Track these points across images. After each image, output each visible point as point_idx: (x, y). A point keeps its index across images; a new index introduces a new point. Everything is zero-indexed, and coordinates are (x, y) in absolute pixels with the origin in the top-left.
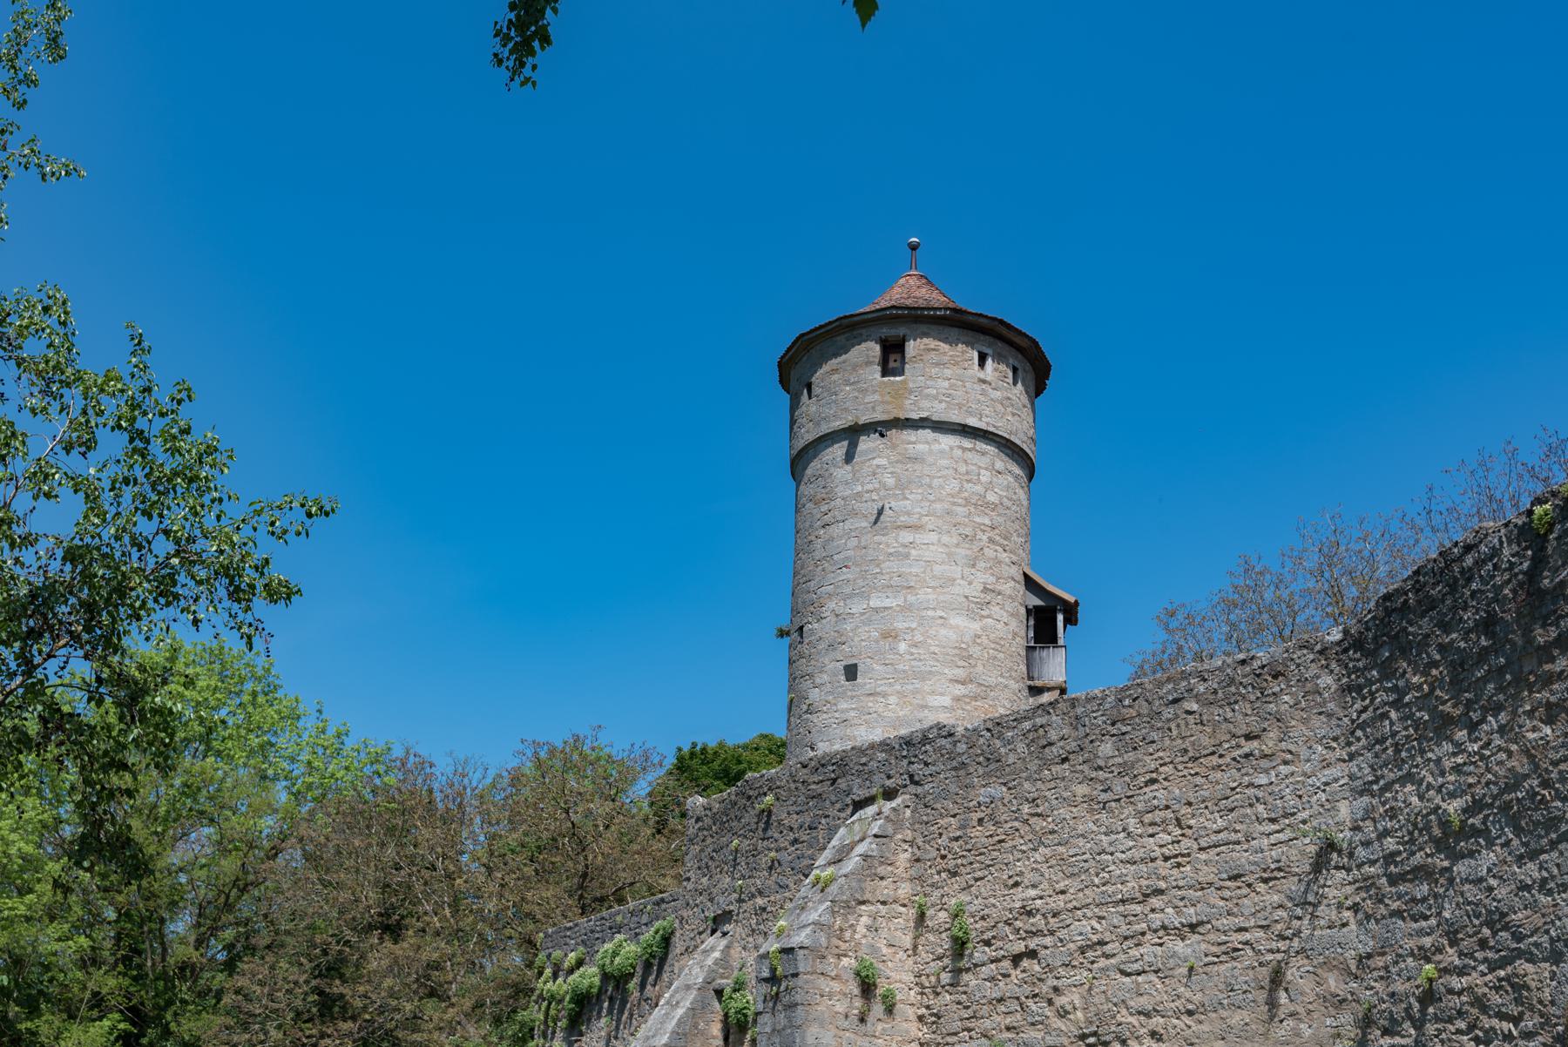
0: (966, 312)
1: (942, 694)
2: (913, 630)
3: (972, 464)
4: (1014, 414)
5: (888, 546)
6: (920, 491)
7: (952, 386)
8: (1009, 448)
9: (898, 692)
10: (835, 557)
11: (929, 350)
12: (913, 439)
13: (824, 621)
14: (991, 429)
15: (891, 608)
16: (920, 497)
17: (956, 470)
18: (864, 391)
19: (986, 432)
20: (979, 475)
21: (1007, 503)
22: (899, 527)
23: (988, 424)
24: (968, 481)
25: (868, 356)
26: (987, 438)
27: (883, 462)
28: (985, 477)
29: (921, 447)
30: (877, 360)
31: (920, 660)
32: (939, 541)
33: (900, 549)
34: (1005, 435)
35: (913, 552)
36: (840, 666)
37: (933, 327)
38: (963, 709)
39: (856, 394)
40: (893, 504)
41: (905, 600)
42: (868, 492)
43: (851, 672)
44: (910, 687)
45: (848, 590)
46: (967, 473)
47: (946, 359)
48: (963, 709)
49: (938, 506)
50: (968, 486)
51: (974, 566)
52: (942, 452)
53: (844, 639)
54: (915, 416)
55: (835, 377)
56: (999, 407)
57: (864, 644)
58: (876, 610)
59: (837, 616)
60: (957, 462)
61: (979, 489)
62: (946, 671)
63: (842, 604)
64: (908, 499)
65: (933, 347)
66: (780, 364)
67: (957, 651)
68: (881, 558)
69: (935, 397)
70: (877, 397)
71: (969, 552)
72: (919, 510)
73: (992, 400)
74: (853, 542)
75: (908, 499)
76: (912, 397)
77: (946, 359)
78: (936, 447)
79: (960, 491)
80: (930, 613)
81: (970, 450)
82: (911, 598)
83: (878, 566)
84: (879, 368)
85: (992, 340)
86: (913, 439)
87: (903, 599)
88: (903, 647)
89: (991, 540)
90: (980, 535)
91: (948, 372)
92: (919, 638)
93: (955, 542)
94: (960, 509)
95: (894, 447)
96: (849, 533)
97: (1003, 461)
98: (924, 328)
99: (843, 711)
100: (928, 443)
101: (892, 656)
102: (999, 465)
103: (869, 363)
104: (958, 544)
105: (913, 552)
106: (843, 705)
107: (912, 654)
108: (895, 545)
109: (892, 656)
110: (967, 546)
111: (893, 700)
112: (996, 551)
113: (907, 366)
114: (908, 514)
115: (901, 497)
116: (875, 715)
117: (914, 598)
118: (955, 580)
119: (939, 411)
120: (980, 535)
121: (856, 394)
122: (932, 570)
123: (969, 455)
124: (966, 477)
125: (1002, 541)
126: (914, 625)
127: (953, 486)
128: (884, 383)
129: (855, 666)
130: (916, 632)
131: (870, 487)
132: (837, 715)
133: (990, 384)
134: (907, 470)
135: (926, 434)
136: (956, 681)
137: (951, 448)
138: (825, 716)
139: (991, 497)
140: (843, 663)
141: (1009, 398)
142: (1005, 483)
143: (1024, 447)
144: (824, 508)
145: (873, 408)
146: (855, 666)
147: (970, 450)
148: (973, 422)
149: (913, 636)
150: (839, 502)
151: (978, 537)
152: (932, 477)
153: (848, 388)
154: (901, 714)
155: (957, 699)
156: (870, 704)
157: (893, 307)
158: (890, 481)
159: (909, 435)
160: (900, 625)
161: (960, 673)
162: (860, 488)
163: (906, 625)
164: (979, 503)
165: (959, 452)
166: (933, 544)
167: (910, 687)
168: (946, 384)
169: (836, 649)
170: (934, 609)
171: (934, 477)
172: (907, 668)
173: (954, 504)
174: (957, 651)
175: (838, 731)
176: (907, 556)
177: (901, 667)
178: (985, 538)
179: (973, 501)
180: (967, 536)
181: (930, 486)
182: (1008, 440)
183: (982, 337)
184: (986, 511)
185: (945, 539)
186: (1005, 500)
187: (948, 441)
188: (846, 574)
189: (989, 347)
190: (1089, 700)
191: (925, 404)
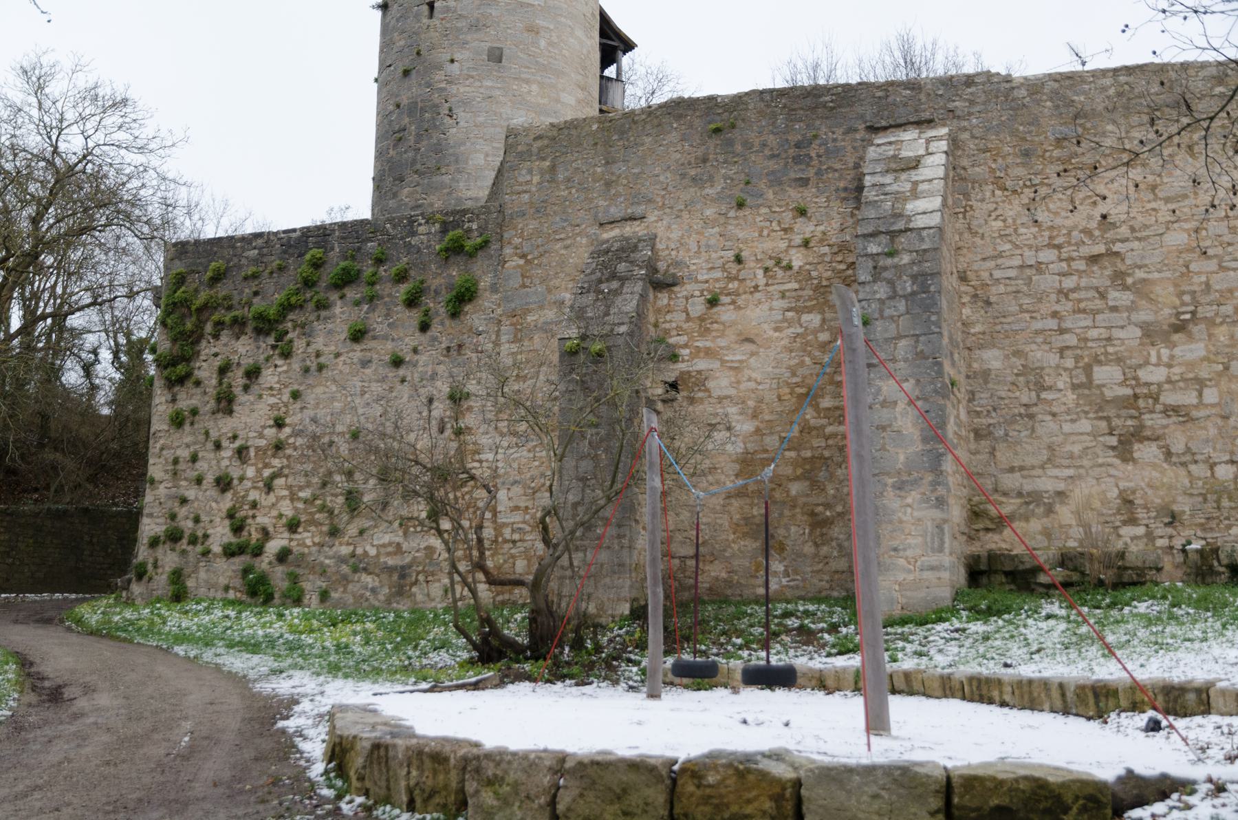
36: (486, 46)
43: (496, 56)
80: (563, 20)
92: (555, 39)
99: (487, 88)
106: (489, 83)
111: (534, 87)
129: (501, 49)
132: (482, 90)
140: (489, 44)
146: (501, 49)
154: (541, 101)
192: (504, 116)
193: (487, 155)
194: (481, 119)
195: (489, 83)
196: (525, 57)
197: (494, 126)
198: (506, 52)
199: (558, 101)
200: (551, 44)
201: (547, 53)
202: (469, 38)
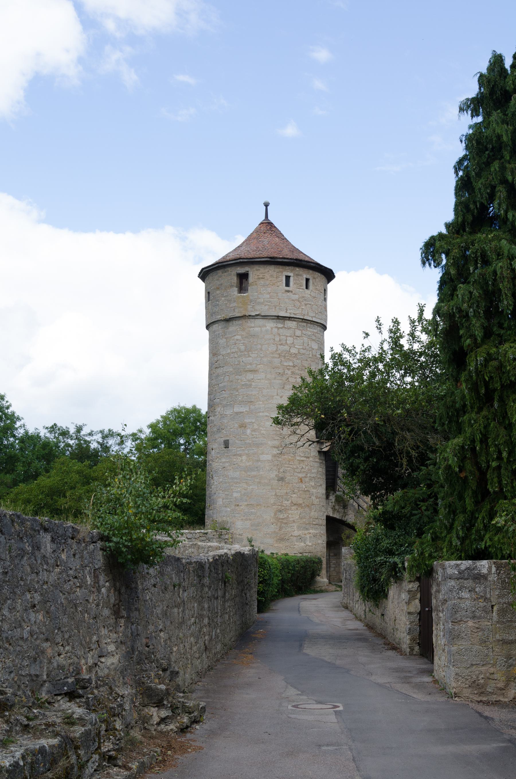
0: (276, 258)
1: (267, 454)
2: (253, 423)
3: (282, 335)
4: (306, 305)
5: (242, 381)
6: (256, 352)
7: (270, 297)
8: (305, 322)
9: (247, 454)
10: (220, 385)
11: (259, 278)
12: (253, 325)
13: (216, 417)
14: (292, 316)
15: (243, 412)
16: (256, 355)
17: (274, 339)
18: (229, 301)
19: (290, 317)
20: (286, 340)
21: (302, 351)
22: (247, 371)
23: (290, 313)
24: (281, 344)
25: (231, 283)
26: (291, 320)
27: (239, 337)
28: (290, 340)
29: (257, 329)
30: (235, 285)
31: (257, 438)
32: (266, 377)
33: (247, 382)
34: (302, 317)
35: (253, 384)
36: (222, 440)
37: (262, 266)
38: (277, 461)
39: (226, 302)
40: (244, 359)
41: (250, 408)
42: (233, 353)
43: (226, 445)
44: (252, 451)
45: (225, 403)
46: (280, 340)
47: (267, 283)
48: (277, 461)
49: (265, 360)
50: (280, 347)
51: (283, 388)
52: (267, 331)
53: (223, 427)
54: (253, 314)
55: (218, 292)
56: (298, 304)
57: (231, 430)
58: (237, 413)
59: (221, 415)
60: (274, 335)
61: (286, 348)
62: (269, 443)
63: (222, 409)
64: (251, 357)
65: (261, 276)
66: (199, 277)
67: (274, 432)
68: (239, 387)
69: (262, 303)
70: (235, 304)
71: (280, 381)
72: (256, 362)
73: (293, 300)
74: (227, 378)
75: (251, 357)
76: (252, 304)
77: (267, 283)
78: (264, 329)
79: (277, 350)
80: (261, 414)
81: (281, 328)
82: (252, 407)
83: (237, 391)
84: (237, 289)
85: (293, 268)
86: (253, 325)
87: (248, 408)
88: (249, 431)
89: (293, 373)
90: (287, 371)
91: (269, 290)
92: (256, 427)
93: (274, 377)
94: (276, 360)
95: (244, 330)
96: (225, 374)
97: (300, 330)
98: (256, 267)
100: (260, 327)
101: (244, 436)
102: (298, 333)
103: (232, 286)
104: (275, 378)
105: (253, 384)
107: (253, 435)
108: (245, 380)
109: (244, 436)
110: (280, 378)
111: (244, 458)
112: (296, 378)
113: (249, 288)
114: (251, 364)
115: (247, 355)
116: (236, 465)
117: (253, 407)
118: (273, 396)
119: (264, 310)
120: (287, 371)
121: (226, 302)
122: (262, 393)
123: (281, 331)
124: (280, 343)
125: (299, 372)
126: (253, 421)
127: (273, 348)
128: (239, 297)
129: (228, 440)
130: (255, 424)
131: (234, 350)
133: (292, 292)
134: (250, 342)
135: (260, 322)
136: (274, 447)
137: (272, 328)
138: (217, 464)
139: (293, 351)
140: (224, 439)
141: (303, 297)
142: (302, 341)
143: (314, 319)
144: (216, 359)
145: (234, 310)
147: (281, 328)
148: (282, 314)
149: (253, 426)
150: (221, 357)
151: (285, 373)
152: (262, 345)
153: (223, 299)
154: (248, 464)
155: (274, 456)
156: (234, 460)
157: (240, 258)
158: (243, 348)
159: (251, 323)
160: (247, 421)
161: (277, 443)
162: (229, 351)
163: (250, 421)
164: (286, 355)
165: (276, 330)
166: (263, 379)
167: (252, 451)
168: (268, 296)
169: (220, 432)
170: (263, 412)
171: (263, 345)
172: (250, 442)
173: (273, 357)
174: (274, 432)
175: (221, 472)
176: (251, 385)
177: (248, 441)
178: (289, 372)
179: (283, 355)
180: (280, 373)
181: (261, 350)
182: (303, 319)
183: (287, 268)
184: (291, 359)
185: (269, 376)
186: (302, 350)
187: (270, 325)
188: (225, 394)
189: (291, 272)
190: (202, 548)
191: (258, 307)
192: (230, 477)
193: (223, 499)
194: (221, 480)
195: (224, 460)
196: (239, 442)
197: (226, 483)
198: (230, 442)
199: (258, 461)
200: (254, 430)
201: (251, 436)
202: (217, 436)
